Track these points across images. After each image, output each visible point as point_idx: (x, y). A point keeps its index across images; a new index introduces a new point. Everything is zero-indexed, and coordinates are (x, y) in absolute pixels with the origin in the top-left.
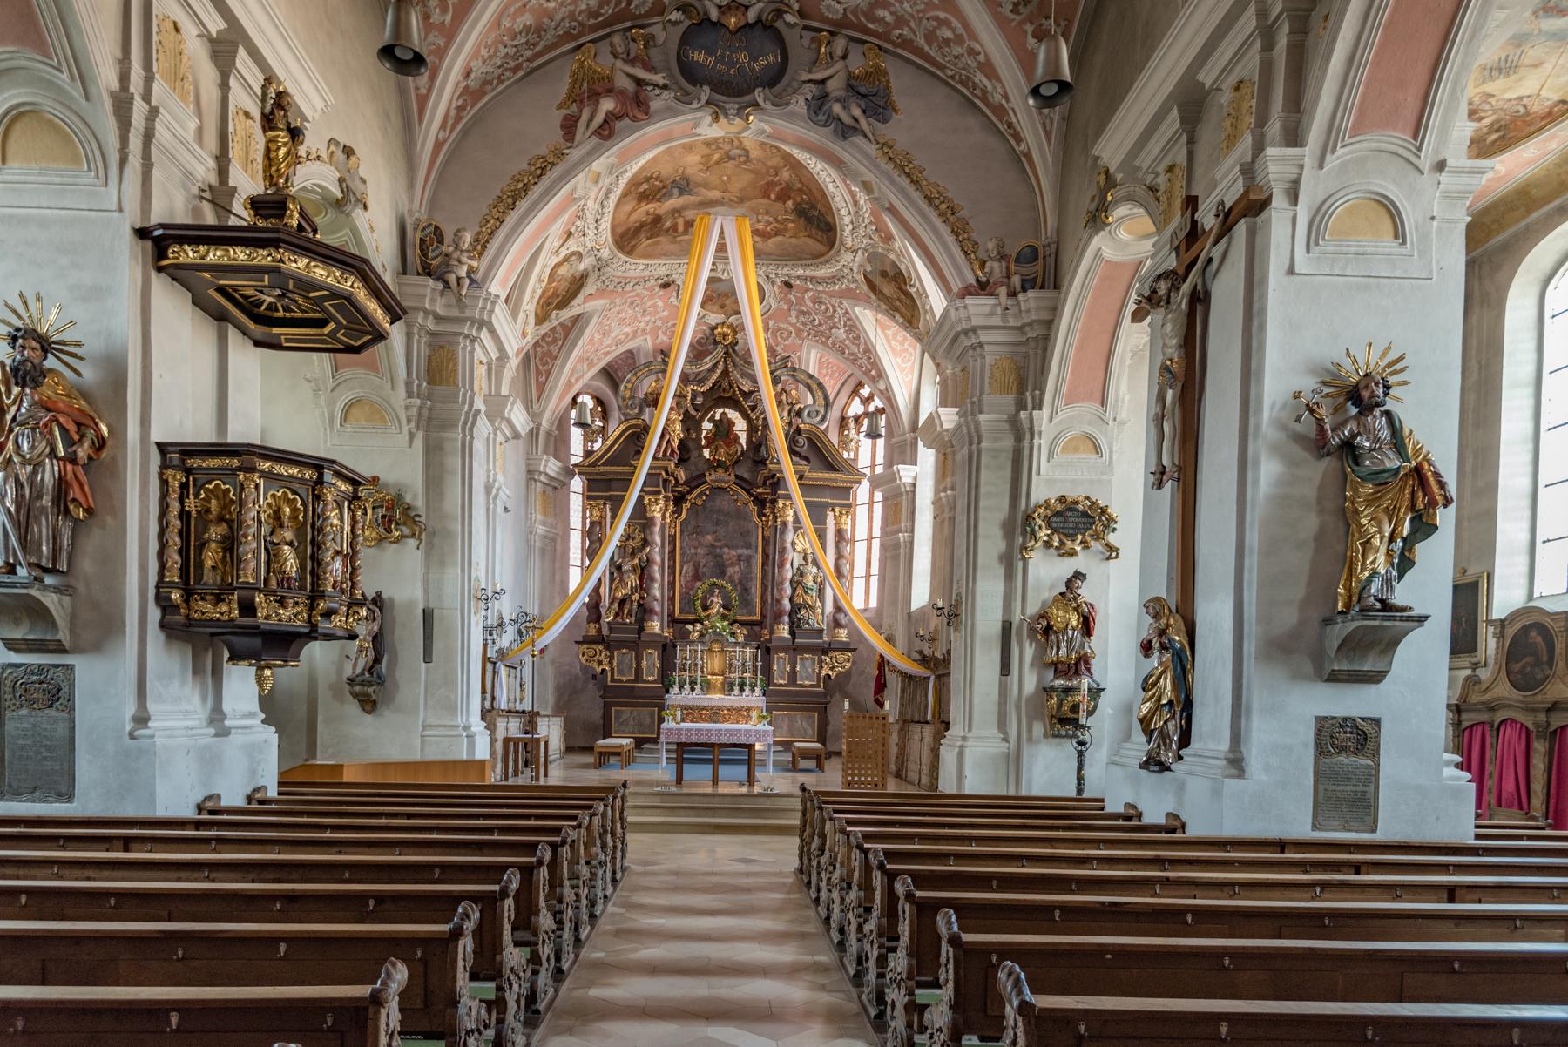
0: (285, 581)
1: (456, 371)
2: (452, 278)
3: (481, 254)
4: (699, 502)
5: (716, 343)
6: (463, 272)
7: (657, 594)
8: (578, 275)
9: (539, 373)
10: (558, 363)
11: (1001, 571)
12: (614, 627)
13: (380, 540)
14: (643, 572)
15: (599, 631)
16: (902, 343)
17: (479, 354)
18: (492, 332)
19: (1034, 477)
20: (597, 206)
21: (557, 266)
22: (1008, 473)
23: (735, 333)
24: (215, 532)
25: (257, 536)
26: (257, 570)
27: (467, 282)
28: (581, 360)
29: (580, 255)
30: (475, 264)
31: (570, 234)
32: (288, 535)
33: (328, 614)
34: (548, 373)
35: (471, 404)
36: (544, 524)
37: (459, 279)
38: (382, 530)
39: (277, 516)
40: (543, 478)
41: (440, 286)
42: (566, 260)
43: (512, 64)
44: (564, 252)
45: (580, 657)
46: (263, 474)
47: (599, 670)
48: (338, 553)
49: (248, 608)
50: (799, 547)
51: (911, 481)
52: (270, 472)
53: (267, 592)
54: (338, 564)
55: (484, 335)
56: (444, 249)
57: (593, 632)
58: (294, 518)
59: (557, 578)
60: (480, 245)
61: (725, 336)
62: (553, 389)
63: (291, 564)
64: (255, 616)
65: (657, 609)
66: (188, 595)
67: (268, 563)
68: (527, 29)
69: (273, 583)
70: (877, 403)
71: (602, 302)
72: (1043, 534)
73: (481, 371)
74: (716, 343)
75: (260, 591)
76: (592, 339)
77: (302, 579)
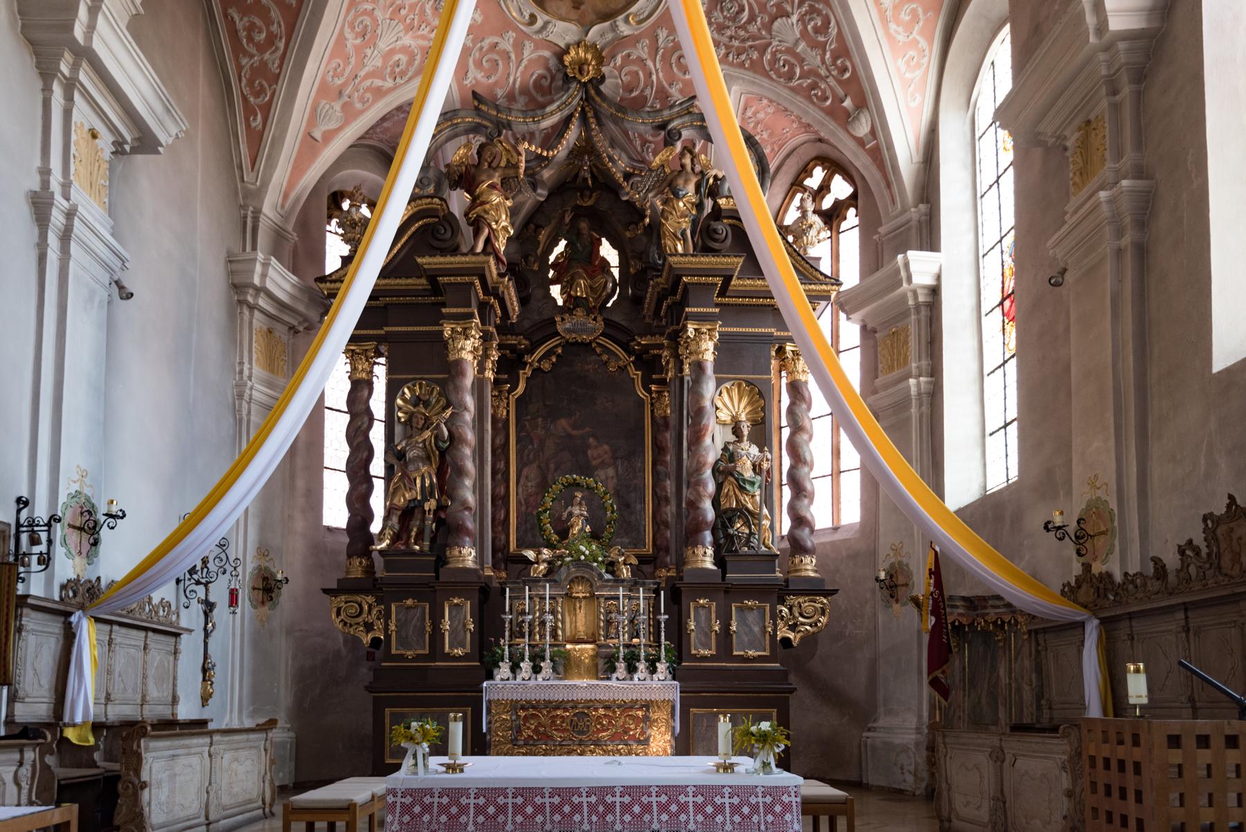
4: (546, 366)
5: (567, 79)
7: (470, 498)
9: (249, 111)
10: (283, 88)
12: (394, 569)
14: (445, 459)
15: (370, 570)
16: (909, 29)
23: (600, 61)
28: (324, 90)
34: (267, 109)
36: (270, 385)
40: (262, 302)
45: (332, 619)
47: (367, 639)
51: (930, 281)
57: (357, 571)
59: (300, 483)
61: (581, 65)
62: (278, 141)
65: (470, 525)
70: (841, 189)
74: (567, 79)
76: (341, 39)
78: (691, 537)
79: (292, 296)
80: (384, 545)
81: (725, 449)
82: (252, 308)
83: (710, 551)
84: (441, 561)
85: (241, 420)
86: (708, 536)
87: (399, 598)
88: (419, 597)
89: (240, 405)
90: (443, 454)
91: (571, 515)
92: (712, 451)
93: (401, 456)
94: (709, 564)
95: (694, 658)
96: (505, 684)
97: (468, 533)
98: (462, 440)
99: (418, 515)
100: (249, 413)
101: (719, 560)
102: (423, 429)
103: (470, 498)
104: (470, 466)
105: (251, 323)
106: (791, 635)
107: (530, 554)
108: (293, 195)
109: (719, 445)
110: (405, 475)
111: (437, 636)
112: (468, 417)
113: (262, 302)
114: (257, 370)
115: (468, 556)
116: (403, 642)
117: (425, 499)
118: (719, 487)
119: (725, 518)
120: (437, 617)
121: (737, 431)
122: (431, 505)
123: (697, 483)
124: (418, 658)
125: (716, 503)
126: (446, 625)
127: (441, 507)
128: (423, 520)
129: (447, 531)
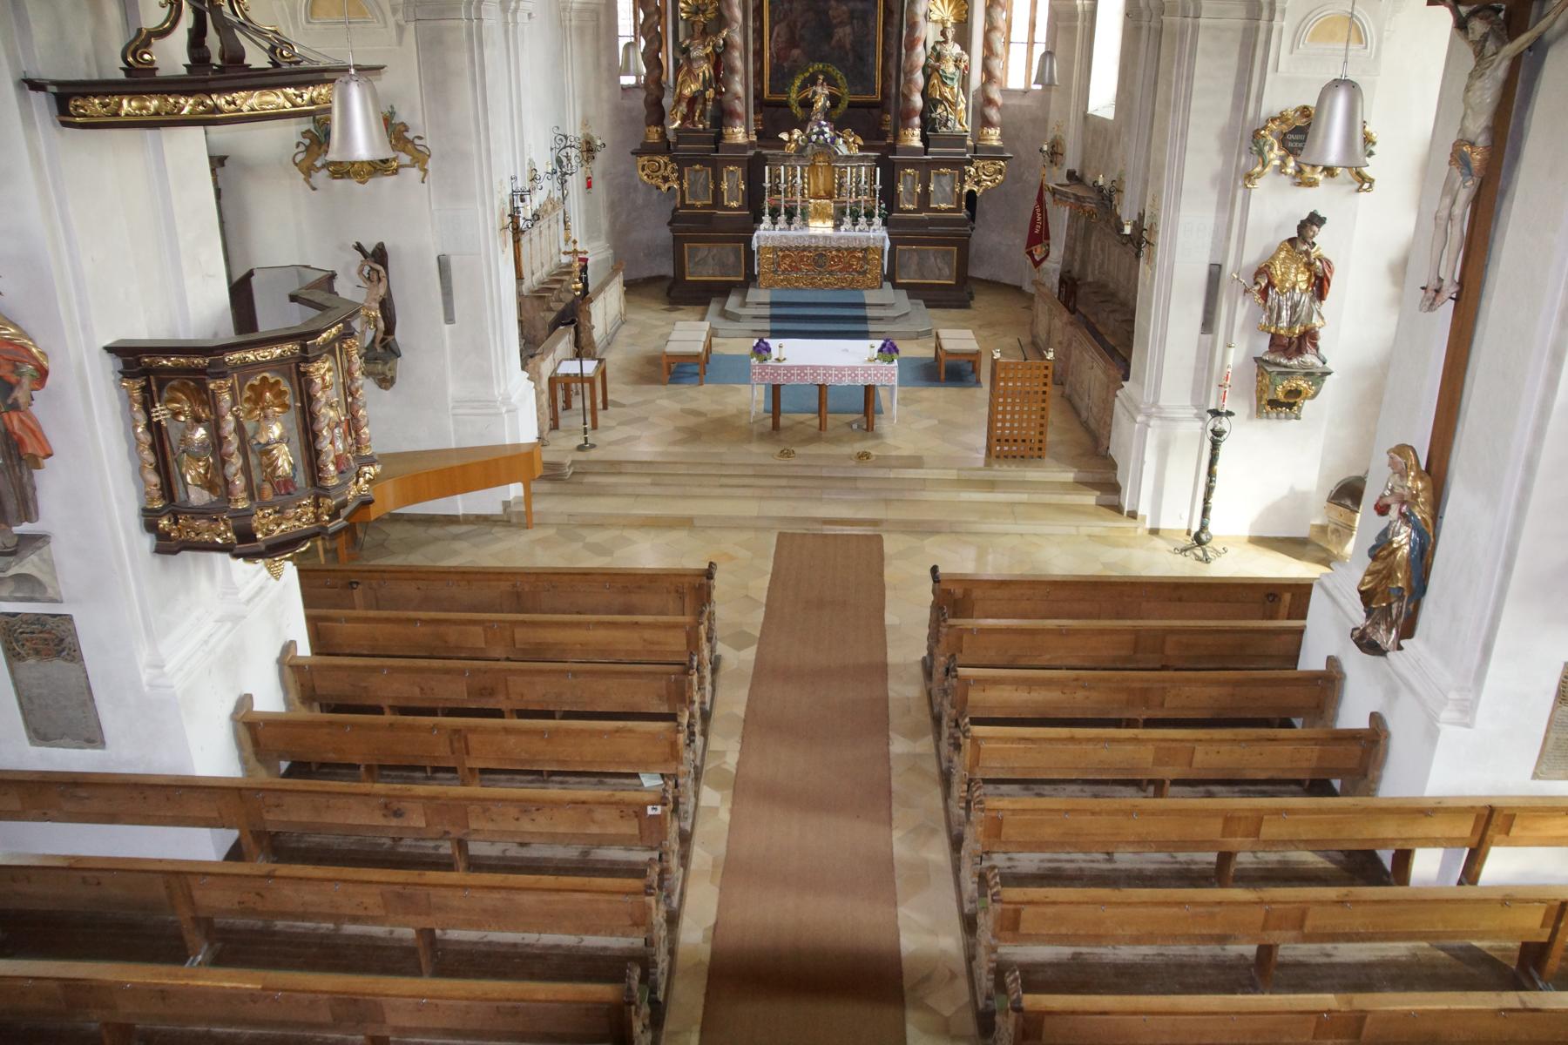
11: (1213, 197)
19: (1270, 76)
22: (1233, 60)
50: (934, 17)
72: (1275, 155)
78: (904, 118)
80: (676, 125)
81: (934, 48)
83: (917, 131)
84: (720, 137)
86: (917, 120)
87: (690, 162)
88: (704, 162)
90: (718, 56)
91: (815, 93)
92: (920, 55)
93: (686, 51)
94: (916, 142)
95: (902, 211)
96: (767, 233)
97: (739, 116)
98: (733, 47)
99: (700, 100)
101: (924, 138)
102: (705, 33)
103: (738, 88)
104: (739, 64)
106: (976, 189)
107: (784, 136)
109: (930, 44)
110: (690, 72)
111: (718, 193)
112: (737, 27)
115: (738, 134)
116: (694, 196)
117: (706, 89)
118: (927, 78)
119: (930, 102)
120: (717, 180)
121: (943, 33)
122: (710, 93)
123: (909, 81)
124: (704, 207)
125: (924, 94)
126: (725, 186)
127: (718, 92)
128: (705, 104)
129: (723, 116)
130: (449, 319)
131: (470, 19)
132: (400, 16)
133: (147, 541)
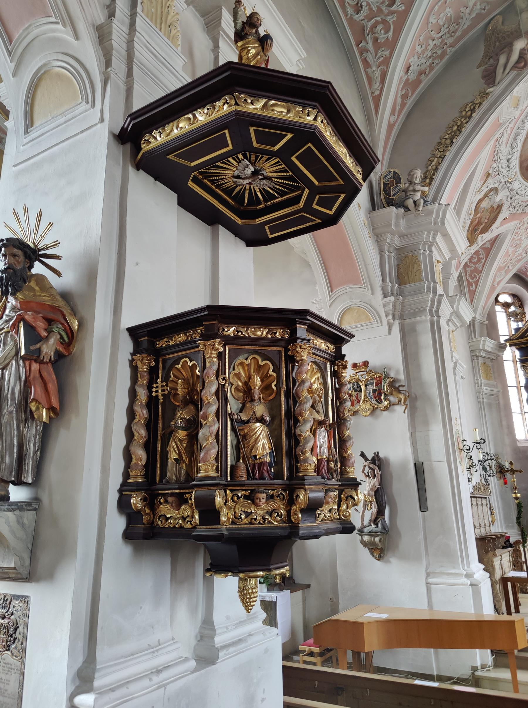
0: (256, 469)
1: (420, 270)
2: (410, 203)
3: (430, 184)
6: (418, 195)
8: (495, 206)
13: (373, 411)
17: (436, 256)
18: (446, 235)
20: (508, 149)
21: (480, 201)
24: (182, 415)
25: (221, 414)
26: (221, 457)
27: (422, 201)
29: (495, 190)
30: (426, 189)
31: (489, 174)
32: (260, 409)
33: (312, 508)
35: (435, 292)
37: (415, 202)
38: (374, 401)
39: (247, 392)
41: (402, 210)
42: (486, 196)
43: (439, 52)
44: (485, 190)
46: (227, 340)
48: (320, 424)
49: (210, 514)
52: (236, 337)
53: (233, 485)
54: (323, 437)
55: (439, 239)
56: (402, 186)
58: (265, 388)
60: (428, 178)
63: (262, 444)
64: (217, 521)
66: (151, 501)
67: (237, 448)
68: (449, 21)
69: (242, 472)
71: (514, 223)
73: (438, 268)
75: (225, 487)
77: (278, 462)
79: (493, 348)
82: (477, 356)
85: (480, 402)
89: (479, 396)
100: (483, 399)
105: (478, 362)
108: (486, 307)
113: (482, 354)
114: (484, 381)
130: (423, 506)
131: (432, 316)
132: (390, 317)
133: (117, 523)
